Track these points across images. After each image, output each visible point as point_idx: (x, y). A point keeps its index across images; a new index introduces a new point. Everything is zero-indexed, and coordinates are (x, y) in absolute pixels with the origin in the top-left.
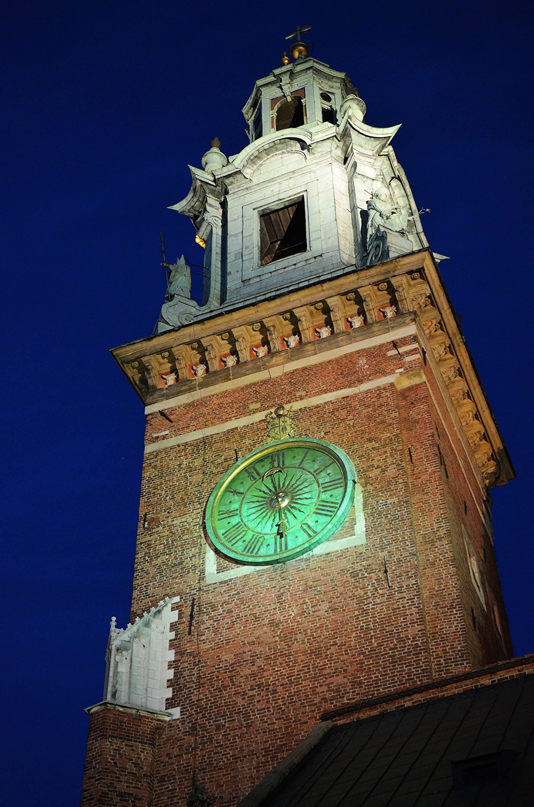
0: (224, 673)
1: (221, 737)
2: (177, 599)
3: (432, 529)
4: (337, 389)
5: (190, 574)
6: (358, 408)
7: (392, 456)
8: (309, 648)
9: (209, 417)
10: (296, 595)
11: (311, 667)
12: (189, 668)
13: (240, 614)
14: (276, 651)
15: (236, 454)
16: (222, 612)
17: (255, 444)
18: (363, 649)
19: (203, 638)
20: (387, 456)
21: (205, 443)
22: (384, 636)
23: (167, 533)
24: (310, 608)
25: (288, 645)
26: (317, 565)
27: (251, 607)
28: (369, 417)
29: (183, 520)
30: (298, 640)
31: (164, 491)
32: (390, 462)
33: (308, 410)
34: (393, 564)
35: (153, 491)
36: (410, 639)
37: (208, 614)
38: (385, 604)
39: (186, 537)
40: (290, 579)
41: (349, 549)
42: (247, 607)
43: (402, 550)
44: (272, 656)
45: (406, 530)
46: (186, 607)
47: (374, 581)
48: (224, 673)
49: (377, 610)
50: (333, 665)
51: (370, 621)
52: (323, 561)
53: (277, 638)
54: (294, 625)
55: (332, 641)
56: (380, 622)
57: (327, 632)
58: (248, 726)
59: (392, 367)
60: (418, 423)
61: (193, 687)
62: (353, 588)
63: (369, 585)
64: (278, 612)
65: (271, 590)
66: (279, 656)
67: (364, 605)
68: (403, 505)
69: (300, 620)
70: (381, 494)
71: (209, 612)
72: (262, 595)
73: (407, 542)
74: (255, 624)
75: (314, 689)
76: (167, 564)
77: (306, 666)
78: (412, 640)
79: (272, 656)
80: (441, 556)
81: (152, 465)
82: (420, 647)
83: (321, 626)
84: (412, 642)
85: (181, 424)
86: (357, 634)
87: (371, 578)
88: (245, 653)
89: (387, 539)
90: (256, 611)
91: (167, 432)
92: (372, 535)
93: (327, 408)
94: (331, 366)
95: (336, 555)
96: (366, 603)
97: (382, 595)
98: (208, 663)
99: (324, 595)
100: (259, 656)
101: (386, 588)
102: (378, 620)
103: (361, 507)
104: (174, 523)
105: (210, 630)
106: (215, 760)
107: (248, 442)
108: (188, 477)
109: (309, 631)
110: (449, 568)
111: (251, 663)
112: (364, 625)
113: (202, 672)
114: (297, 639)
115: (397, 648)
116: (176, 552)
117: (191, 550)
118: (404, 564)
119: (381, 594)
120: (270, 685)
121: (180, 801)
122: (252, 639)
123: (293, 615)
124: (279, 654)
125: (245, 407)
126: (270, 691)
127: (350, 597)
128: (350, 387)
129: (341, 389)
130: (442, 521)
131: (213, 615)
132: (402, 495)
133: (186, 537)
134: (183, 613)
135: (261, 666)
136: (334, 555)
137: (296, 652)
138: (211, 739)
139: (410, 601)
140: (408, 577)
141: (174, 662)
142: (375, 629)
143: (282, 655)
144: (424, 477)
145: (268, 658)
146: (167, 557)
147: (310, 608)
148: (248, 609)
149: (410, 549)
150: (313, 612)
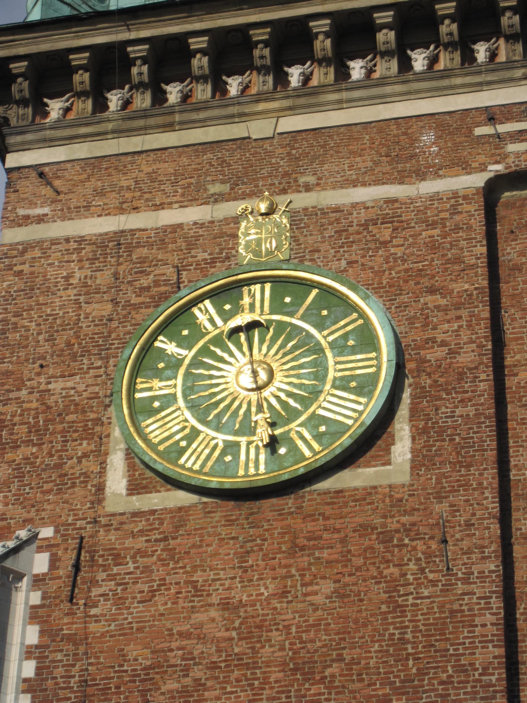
0: (130, 681)
2: (47, 532)
5: (76, 489)
6: (413, 225)
7: (469, 326)
8: (291, 659)
9: (128, 195)
10: (274, 558)
12: (65, 663)
13: (167, 578)
14: (231, 655)
15: (179, 274)
16: (132, 570)
17: (213, 262)
18: (391, 676)
19: (93, 611)
20: (461, 326)
21: (119, 244)
22: (430, 657)
23: (34, 405)
24: (299, 588)
25: (253, 648)
26: (316, 509)
27: (188, 569)
29: (70, 384)
30: (273, 642)
31: (33, 324)
33: (319, 213)
34: (458, 528)
35: (14, 320)
36: (477, 669)
37: (105, 568)
38: (436, 600)
39: (71, 417)
40: (265, 527)
41: (380, 489)
42: (181, 568)
43: (475, 505)
44: (223, 665)
45: (485, 469)
46: (66, 549)
47: (420, 555)
48: (130, 681)
49: (423, 609)
50: (333, 696)
51: (407, 627)
52: (328, 504)
53: (234, 634)
54: (268, 615)
55: (335, 653)
56: (426, 630)
57: (326, 635)
59: (482, 158)
60: (520, 270)
62: (381, 562)
63: (410, 560)
64: (239, 585)
65: (227, 543)
66: (236, 666)
67: (399, 596)
68: (484, 422)
69: (278, 606)
70: (444, 396)
71: (110, 564)
72: (209, 549)
73: (486, 491)
74: (193, 601)
76: (32, 463)
77: (283, 692)
78: (480, 671)
79: (223, 665)
81: (15, 268)
82: (494, 686)
84: (480, 675)
86: (382, 646)
87: (415, 548)
88: (171, 650)
89: (450, 482)
90: (199, 577)
92: (423, 469)
93: (355, 215)
94: (367, 137)
96: (402, 593)
97: (434, 583)
98: (102, 660)
99: (326, 567)
100: (197, 660)
101: (442, 571)
102: (422, 627)
104: (50, 387)
105: (109, 600)
107: (202, 256)
108: (83, 304)
109: (294, 629)
111: (182, 671)
112: (397, 632)
113: (89, 675)
114: (270, 640)
115: (452, 682)
116: (51, 442)
117: (81, 444)
118: (477, 532)
119: (431, 581)
122: (185, 628)
123: (266, 594)
124: (236, 662)
125: (200, 187)
127: (374, 578)
128: (401, 183)
129: (383, 184)
131: (115, 571)
132: (482, 404)
133: (71, 417)
134: (59, 560)
135: (201, 679)
136: (350, 496)
137: (268, 664)
139: (483, 602)
140: (483, 558)
141: (37, 647)
142: (414, 643)
143: (240, 665)
145: (214, 666)
146: (34, 450)
147: (299, 588)
148: (181, 571)
149: (490, 506)
150: (306, 595)
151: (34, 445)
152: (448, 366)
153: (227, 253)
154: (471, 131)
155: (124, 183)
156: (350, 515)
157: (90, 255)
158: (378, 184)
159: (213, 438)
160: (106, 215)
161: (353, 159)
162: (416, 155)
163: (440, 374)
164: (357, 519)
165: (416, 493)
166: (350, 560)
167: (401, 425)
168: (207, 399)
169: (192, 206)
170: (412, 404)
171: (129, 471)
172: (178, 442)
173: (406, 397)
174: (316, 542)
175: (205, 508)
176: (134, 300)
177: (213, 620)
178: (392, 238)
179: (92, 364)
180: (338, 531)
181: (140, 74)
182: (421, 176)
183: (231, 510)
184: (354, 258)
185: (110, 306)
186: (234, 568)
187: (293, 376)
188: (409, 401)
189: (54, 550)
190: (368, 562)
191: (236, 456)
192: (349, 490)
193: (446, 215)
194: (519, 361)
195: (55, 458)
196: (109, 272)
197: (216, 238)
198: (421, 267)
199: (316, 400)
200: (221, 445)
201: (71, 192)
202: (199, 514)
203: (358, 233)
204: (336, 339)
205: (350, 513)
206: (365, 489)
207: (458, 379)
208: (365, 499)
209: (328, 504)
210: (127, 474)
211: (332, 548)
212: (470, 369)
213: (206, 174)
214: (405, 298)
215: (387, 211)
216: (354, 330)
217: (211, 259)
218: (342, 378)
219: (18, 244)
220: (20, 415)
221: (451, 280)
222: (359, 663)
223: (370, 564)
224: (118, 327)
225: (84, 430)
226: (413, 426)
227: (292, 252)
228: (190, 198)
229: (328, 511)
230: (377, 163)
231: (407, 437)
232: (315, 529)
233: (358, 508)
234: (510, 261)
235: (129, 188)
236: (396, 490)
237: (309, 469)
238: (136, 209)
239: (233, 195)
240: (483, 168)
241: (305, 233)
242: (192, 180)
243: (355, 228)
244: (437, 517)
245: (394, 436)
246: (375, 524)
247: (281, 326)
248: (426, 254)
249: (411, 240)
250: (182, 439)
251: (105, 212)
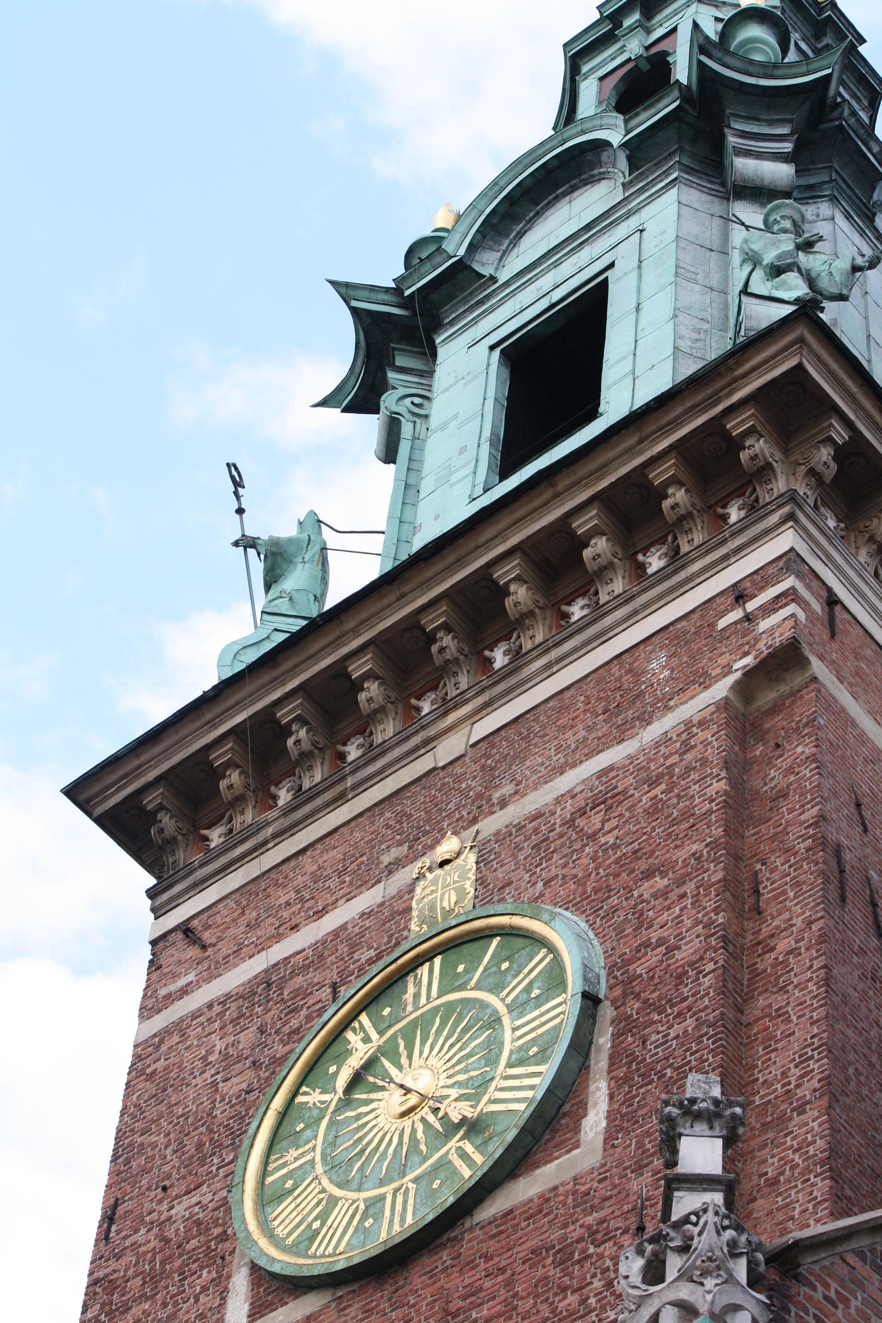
3: (783, 1086)
4: (589, 756)
6: (631, 792)
7: (696, 902)
26: (478, 1251)
28: (655, 810)
29: (194, 1200)
32: (688, 923)
39: (194, 1243)
52: (494, 1236)
63: (594, 1276)
70: (656, 1017)
80: (797, 1157)
85: (225, 948)
91: (191, 977)
93: (559, 812)
94: (582, 698)
95: (525, 1212)
104: (173, 1212)
110: (813, 1185)
116: (167, 1287)
130: (812, 1057)
132: (706, 1007)
136: (521, 1215)
144: (783, 945)
151: (147, 1298)
152: (663, 973)
153: (396, 939)
154: (712, 625)
155: (282, 900)
156: (520, 1242)
157: (235, 1015)
158: (592, 756)
159: (354, 1202)
160: (258, 952)
161: (562, 737)
162: (642, 693)
163: (653, 988)
164: (529, 1244)
165: (608, 1174)
166: (515, 1308)
167: (596, 1085)
168: (351, 1149)
169: (361, 893)
170: (612, 1047)
171: (253, 1290)
172: (310, 1225)
173: (604, 1041)
174: (475, 1298)
175: (340, 1304)
176: (280, 1050)
178: (603, 823)
179: (223, 1160)
180: (502, 1270)
181: (298, 742)
182: (646, 720)
183: (371, 1296)
184: (554, 871)
185: (250, 1074)
187: (459, 1072)
188: (609, 1045)
190: (539, 1301)
191: (378, 1217)
193: (675, 759)
194: (777, 927)
195: (170, 1307)
196: (255, 1028)
197: (384, 924)
198: (637, 847)
199: (485, 1093)
200: (362, 1206)
202: (331, 1316)
203: (561, 836)
204: (517, 997)
205: (521, 1238)
206: (541, 1196)
207: (676, 985)
208: (540, 1211)
209: (494, 1236)
210: (250, 1295)
211: (494, 1298)
212: (692, 964)
214: (613, 900)
215: (600, 788)
216: (541, 972)
217: (376, 955)
218: (520, 1048)
219: (155, 1036)
220: (135, 1265)
221: (676, 847)
223: (541, 1303)
224: (259, 1097)
225: (205, 1256)
226: (612, 1079)
227: (477, 900)
228: (359, 883)
230: (589, 729)
231: (602, 1098)
232: (474, 1278)
233: (531, 1226)
234: (772, 789)
235: (288, 904)
236: (582, 1181)
237: (460, 1194)
238: (295, 928)
239: (411, 855)
240: (727, 670)
241: (495, 866)
242: (364, 858)
243: (558, 830)
244: (635, 1197)
245: (586, 1104)
246: (552, 1241)
248: (645, 825)
249: (627, 814)
250: (316, 1219)
251: (261, 947)
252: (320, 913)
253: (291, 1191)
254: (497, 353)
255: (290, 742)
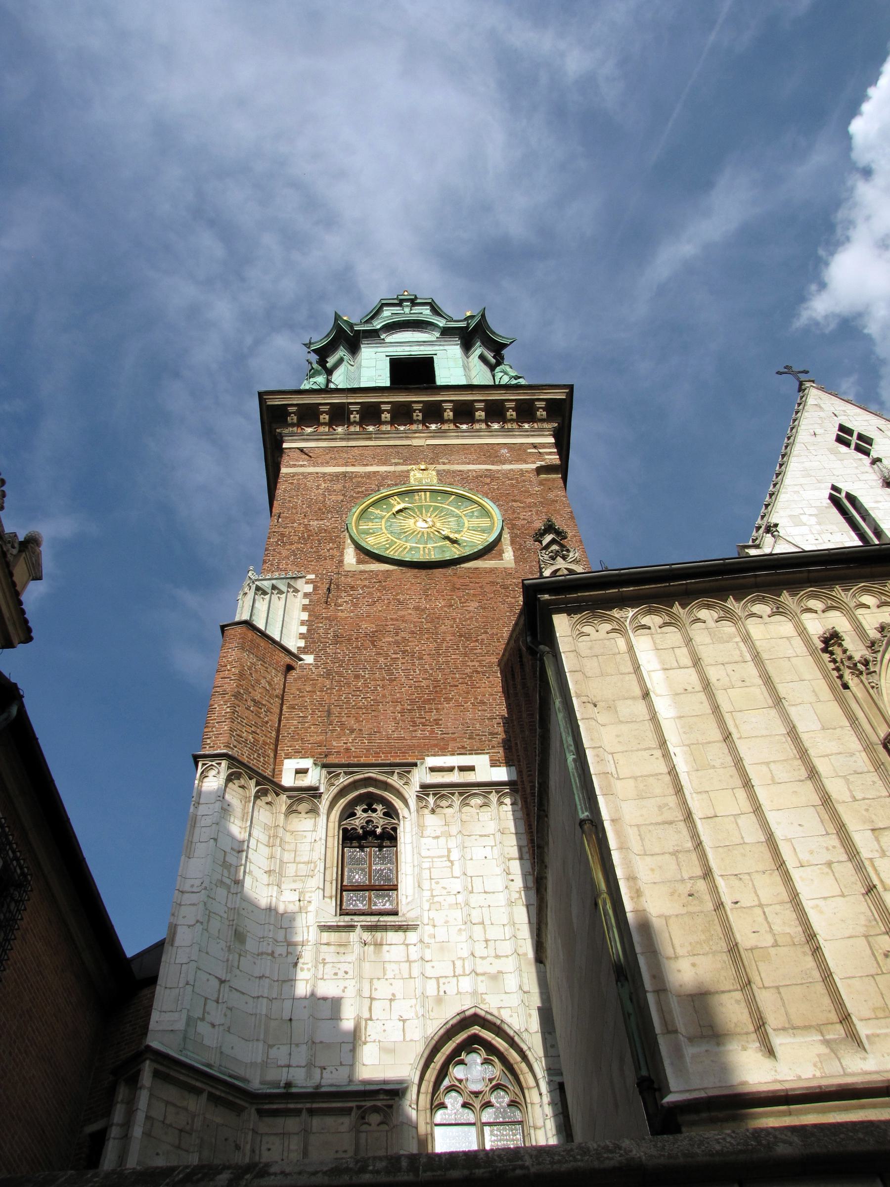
1: (360, 684)
2: (312, 576)
4: (480, 464)
11: (460, 645)
23: (302, 529)
58: (391, 680)
61: (328, 642)
75: (464, 663)
79: (418, 632)
83: (471, 618)
90: (402, 598)
91: (305, 463)
93: (470, 473)
103: (508, 542)
106: (354, 701)
109: (458, 620)
120: (415, 653)
121: (312, 727)
126: (416, 658)
131: (352, 593)
138: (348, 684)
141: (307, 621)
145: (413, 633)
164: (487, 579)
176: (355, 495)
177: (411, 614)
180: (478, 583)
181: (355, 417)
186: (421, 594)
189: (316, 583)
192: (482, 568)
200: (409, 547)
201: (318, 457)
206: (491, 568)
213: (391, 455)
222: (497, 635)
229: (471, 575)
240: (534, 463)
247: (436, 508)
252: (367, 465)
253: (372, 534)
254: (388, 358)
255: (352, 416)
